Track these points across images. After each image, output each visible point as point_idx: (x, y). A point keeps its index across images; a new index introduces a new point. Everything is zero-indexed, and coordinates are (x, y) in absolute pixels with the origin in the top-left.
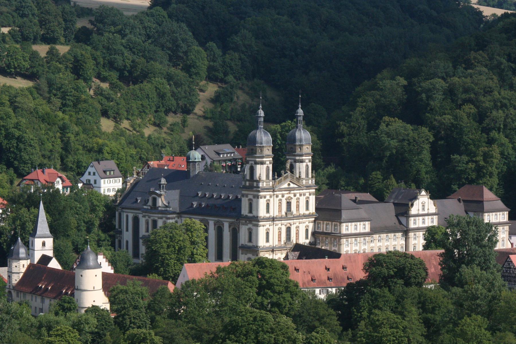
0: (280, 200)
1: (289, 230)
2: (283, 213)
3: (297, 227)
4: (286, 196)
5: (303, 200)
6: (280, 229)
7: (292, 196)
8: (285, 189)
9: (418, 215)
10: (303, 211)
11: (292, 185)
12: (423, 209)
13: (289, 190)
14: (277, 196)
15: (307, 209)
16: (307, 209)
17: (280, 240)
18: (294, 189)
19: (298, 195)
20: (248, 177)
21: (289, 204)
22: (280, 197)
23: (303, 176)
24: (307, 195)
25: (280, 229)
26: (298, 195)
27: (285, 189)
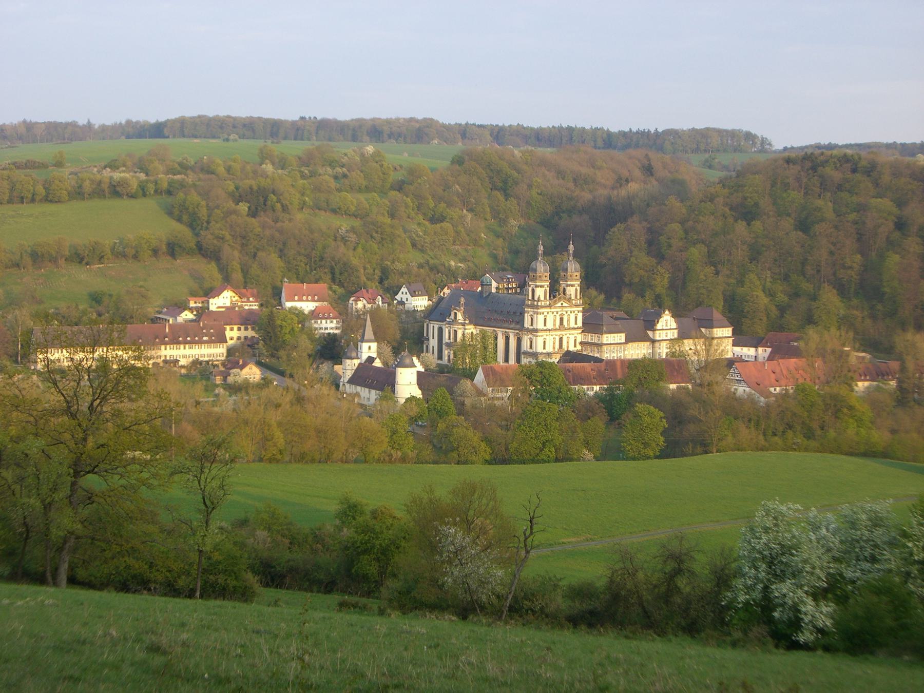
1: (561, 339)
2: (557, 327)
3: (568, 337)
7: (564, 313)
10: (572, 325)
11: (565, 304)
12: (666, 326)
13: (562, 306)
14: (553, 313)
15: (576, 324)
17: (554, 348)
20: (530, 298)
21: (562, 319)
22: (555, 313)
23: (573, 297)
24: (576, 312)
25: (554, 338)
26: (569, 313)
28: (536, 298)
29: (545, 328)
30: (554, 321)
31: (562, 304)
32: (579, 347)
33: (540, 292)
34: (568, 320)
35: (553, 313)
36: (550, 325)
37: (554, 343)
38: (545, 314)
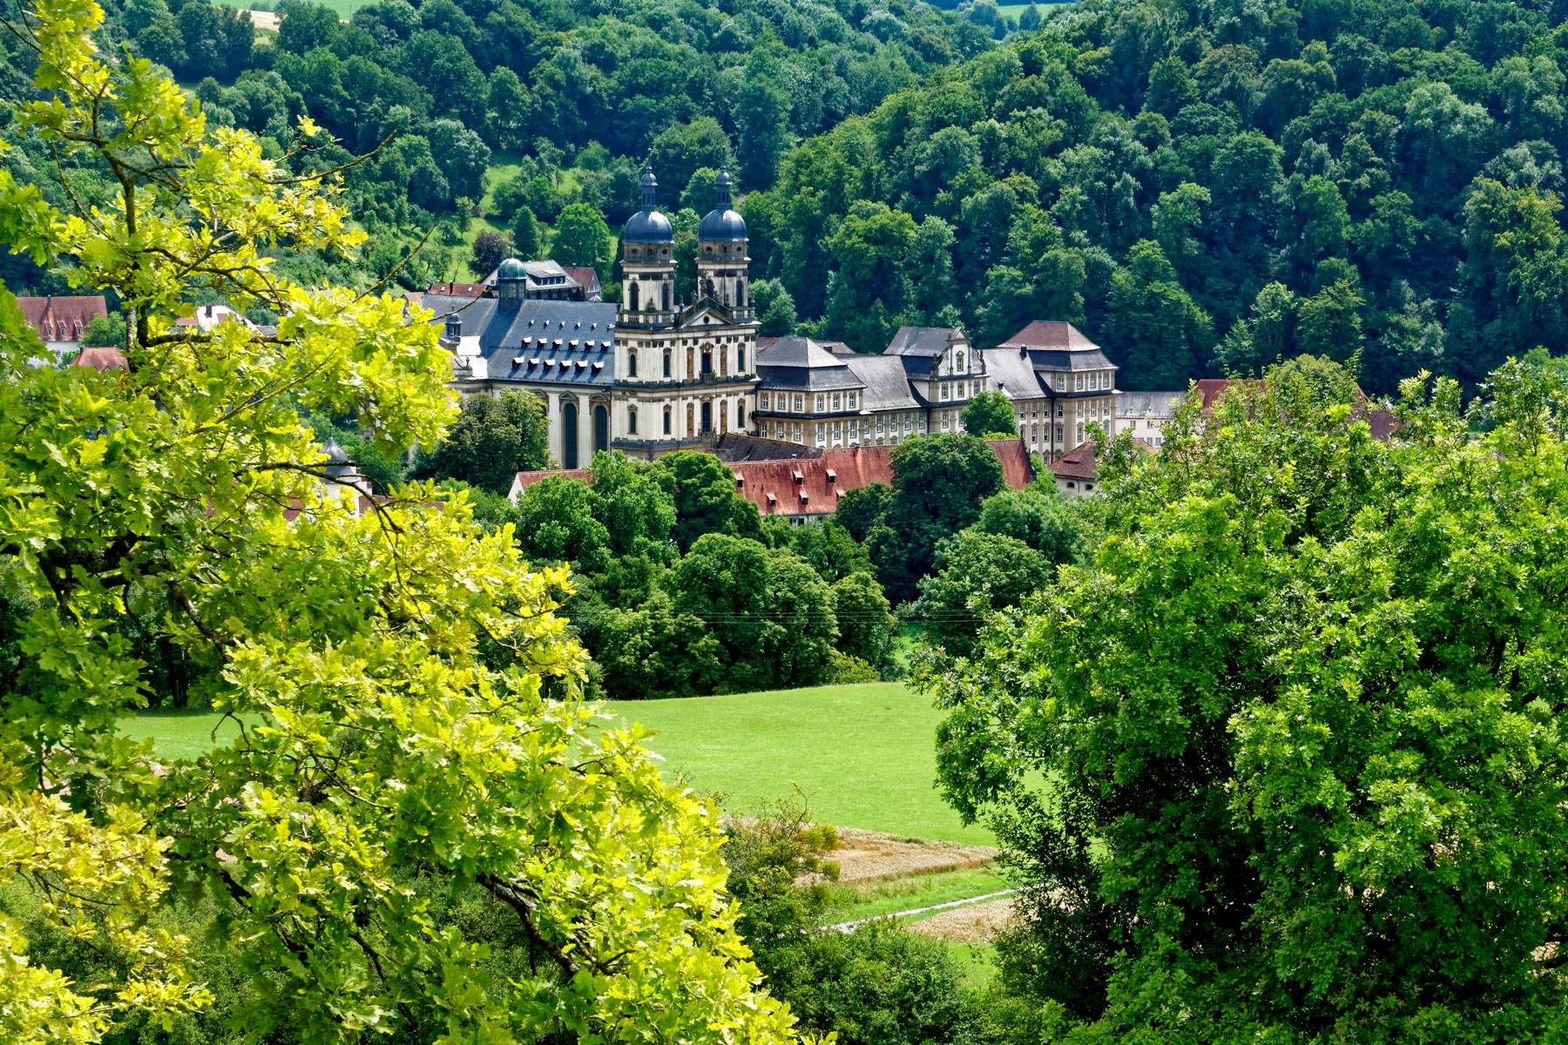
0: (691, 350)
1: (707, 409)
2: (697, 376)
3: (724, 403)
4: (701, 342)
5: (733, 349)
6: (690, 406)
7: (712, 341)
8: (699, 328)
9: (951, 378)
10: (733, 371)
11: (712, 321)
12: (960, 367)
13: (707, 328)
14: (685, 343)
15: (741, 368)
16: (741, 368)
17: (690, 429)
18: (715, 327)
19: (724, 340)
20: (627, 305)
21: (706, 358)
22: (690, 343)
23: (733, 302)
24: (741, 339)
25: (690, 406)
26: (724, 340)
27: (699, 328)
28: (642, 307)
29: (667, 380)
30: (690, 362)
31: (706, 320)
32: (750, 426)
33: (650, 292)
34: (723, 361)
35: (685, 343)
36: (679, 373)
37: (690, 419)
38: (667, 344)
